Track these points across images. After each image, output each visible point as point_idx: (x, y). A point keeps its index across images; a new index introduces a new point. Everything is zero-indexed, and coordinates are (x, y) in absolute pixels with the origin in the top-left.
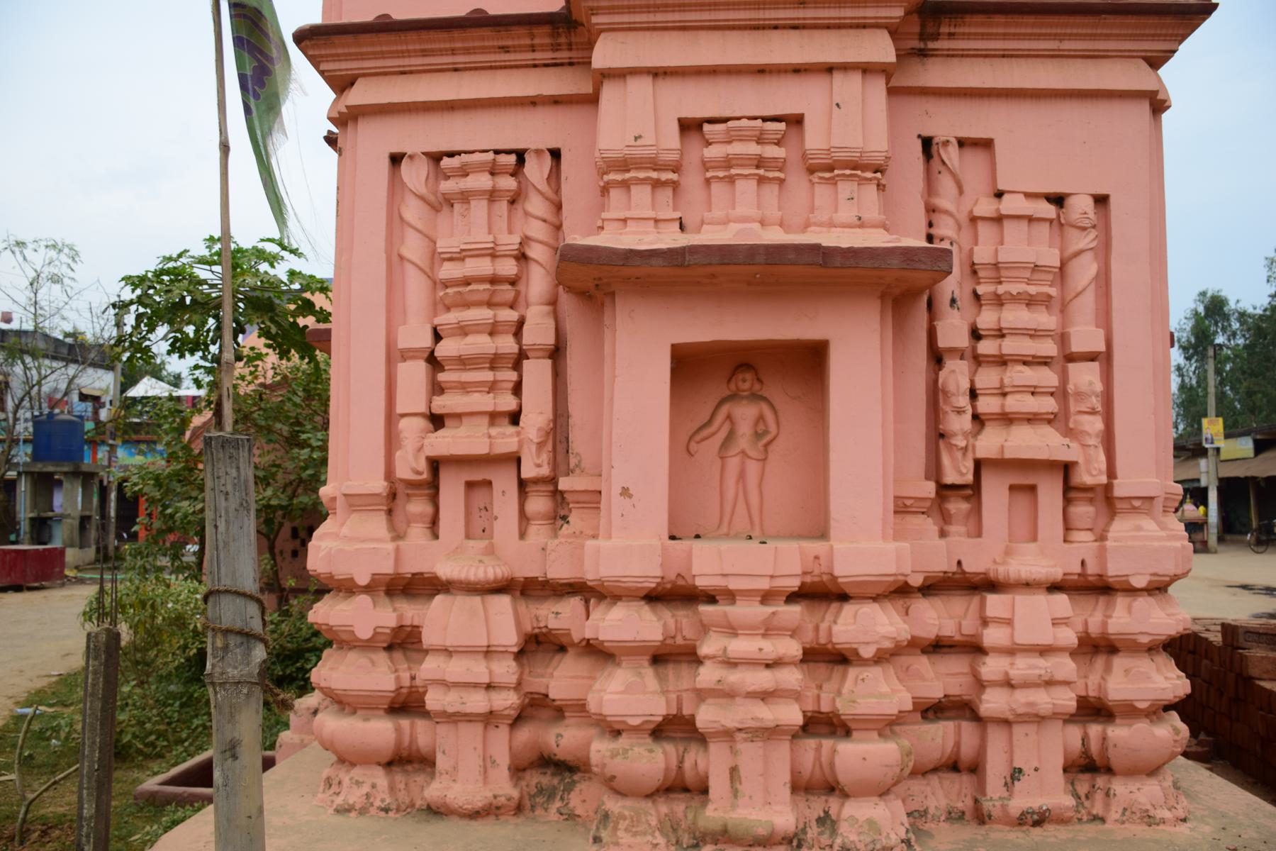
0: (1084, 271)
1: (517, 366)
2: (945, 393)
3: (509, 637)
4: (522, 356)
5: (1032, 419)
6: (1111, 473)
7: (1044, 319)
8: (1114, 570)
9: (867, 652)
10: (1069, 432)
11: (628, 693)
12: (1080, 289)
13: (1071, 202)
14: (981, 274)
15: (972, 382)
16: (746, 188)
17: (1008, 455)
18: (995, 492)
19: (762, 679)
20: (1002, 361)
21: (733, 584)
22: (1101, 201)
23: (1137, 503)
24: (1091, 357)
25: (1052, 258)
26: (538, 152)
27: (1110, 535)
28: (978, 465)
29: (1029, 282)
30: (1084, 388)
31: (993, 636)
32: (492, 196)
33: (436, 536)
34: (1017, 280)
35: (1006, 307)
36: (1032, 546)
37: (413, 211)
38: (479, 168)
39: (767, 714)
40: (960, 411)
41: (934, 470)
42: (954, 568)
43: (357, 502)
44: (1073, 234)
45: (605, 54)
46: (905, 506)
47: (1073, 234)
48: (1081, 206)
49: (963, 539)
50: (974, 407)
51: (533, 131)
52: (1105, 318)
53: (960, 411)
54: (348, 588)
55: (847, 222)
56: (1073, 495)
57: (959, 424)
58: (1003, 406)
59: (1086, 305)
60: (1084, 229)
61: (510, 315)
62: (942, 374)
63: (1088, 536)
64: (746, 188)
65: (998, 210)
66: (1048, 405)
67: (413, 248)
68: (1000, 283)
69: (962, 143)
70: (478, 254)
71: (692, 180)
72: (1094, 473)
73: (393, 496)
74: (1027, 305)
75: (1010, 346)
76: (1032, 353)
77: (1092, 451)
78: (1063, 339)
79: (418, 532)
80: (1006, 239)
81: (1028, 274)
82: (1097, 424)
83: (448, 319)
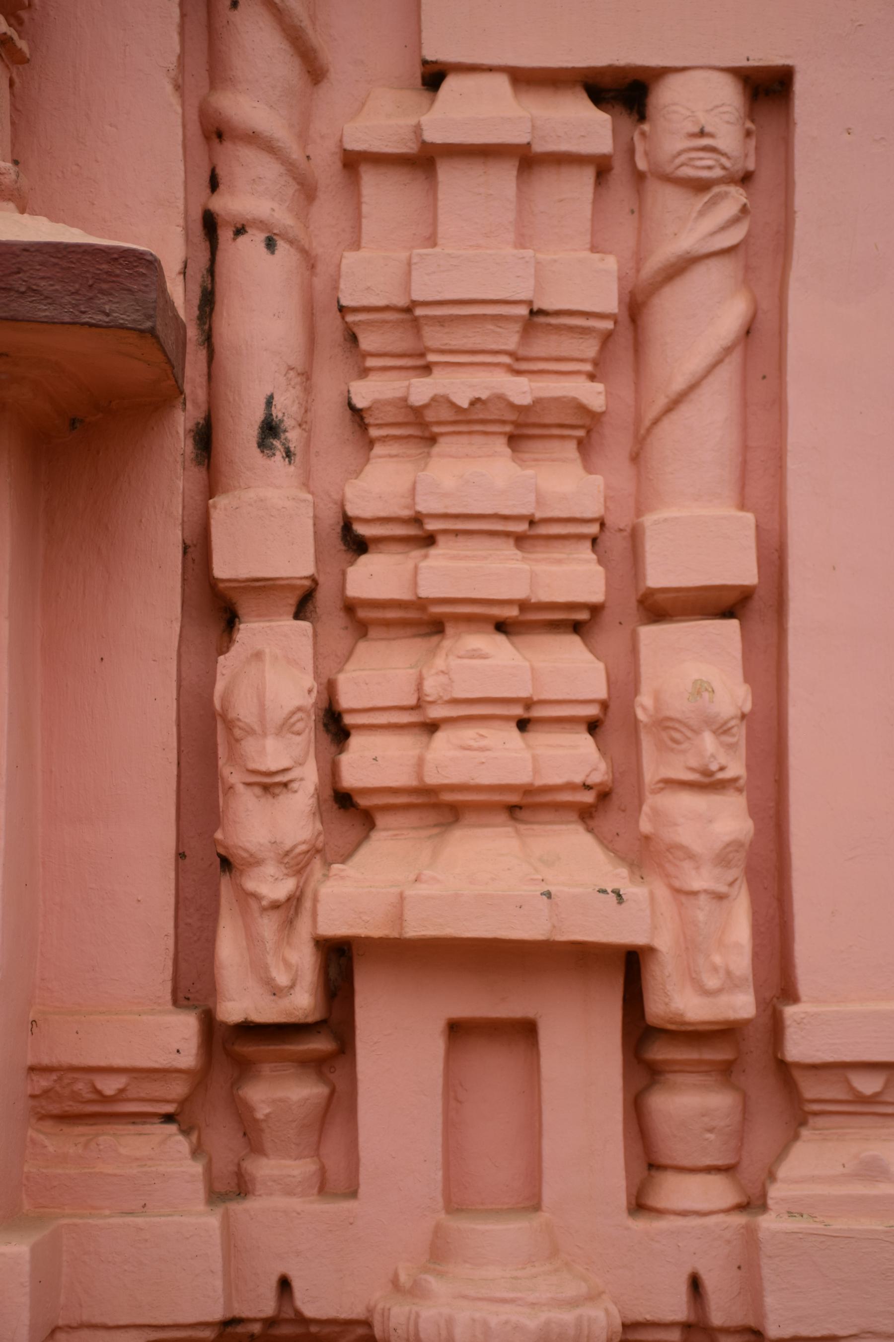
0: (701, 322)
2: (230, 725)
5: (521, 805)
6: (779, 982)
7: (565, 484)
10: (645, 855)
12: (679, 384)
13: (668, 97)
14: (367, 342)
15: (330, 689)
17: (414, 930)
18: (399, 1045)
20: (429, 621)
22: (767, 90)
23: (868, 1084)
24: (729, 604)
25: (590, 284)
27: (775, 1192)
28: (339, 958)
29: (518, 363)
30: (679, 706)
34: (474, 358)
35: (444, 446)
36: (512, 1231)
40: (271, 785)
41: (193, 984)
42: (265, 1304)
44: (668, 201)
46: (105, 1099)
47: (668, 201)
48: (699, 109)
49: (295, 1203)
50: (332, 771)
52: (761, 475)
53: (271, 785)
56: (660, 1053)
57: (272, 826)
58: (420, 763)
59: (701, 437)
60: (700, 186)
62: (227, 663)
63: (715, 1192)
65: (418, 129)
66: (572, 759)
68: (427, 369)
72: (712, 982)
74: (513, 440)
76: (519, 592)
77: (702, 911)
78: (613, 539)
80: (447, 225)
81: (510, 339)
82: (728, 820)
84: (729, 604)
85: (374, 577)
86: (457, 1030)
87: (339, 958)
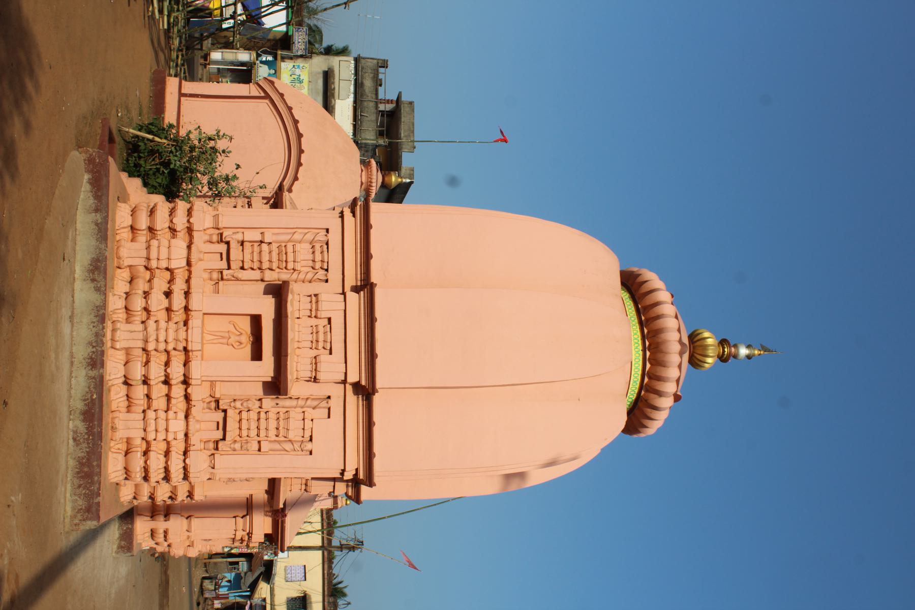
0: (288, 446)
1: (260, 269)
3: (173, 266)
7: (272, 433)
8: (191, 454)
16: (310, 337)
19: (162, 339)
21: (189, 331)
24: (259, 450)
25: (291, 435)
26: (326, 275)
31: (171, 413)
32: (314, 261)
37: (309, 237)
38: (323, 257)
39: (152, 338)
43: (216, 217)
45: (352, 297)
48: (309, 446)
51: (335, 275)
54: (190, 212)
57: (238, 404)
61: (274, 266)
64: (310, 337)
67: (297, 237)
69: (329, 409)
70: (295, 257)
71: (314, 321)
73: (218, 229)
75: (263, 421)
83: (274, 246)
84: (259, 450)
85: (263, 415)
86: (218, 423)
87: (225, 411)
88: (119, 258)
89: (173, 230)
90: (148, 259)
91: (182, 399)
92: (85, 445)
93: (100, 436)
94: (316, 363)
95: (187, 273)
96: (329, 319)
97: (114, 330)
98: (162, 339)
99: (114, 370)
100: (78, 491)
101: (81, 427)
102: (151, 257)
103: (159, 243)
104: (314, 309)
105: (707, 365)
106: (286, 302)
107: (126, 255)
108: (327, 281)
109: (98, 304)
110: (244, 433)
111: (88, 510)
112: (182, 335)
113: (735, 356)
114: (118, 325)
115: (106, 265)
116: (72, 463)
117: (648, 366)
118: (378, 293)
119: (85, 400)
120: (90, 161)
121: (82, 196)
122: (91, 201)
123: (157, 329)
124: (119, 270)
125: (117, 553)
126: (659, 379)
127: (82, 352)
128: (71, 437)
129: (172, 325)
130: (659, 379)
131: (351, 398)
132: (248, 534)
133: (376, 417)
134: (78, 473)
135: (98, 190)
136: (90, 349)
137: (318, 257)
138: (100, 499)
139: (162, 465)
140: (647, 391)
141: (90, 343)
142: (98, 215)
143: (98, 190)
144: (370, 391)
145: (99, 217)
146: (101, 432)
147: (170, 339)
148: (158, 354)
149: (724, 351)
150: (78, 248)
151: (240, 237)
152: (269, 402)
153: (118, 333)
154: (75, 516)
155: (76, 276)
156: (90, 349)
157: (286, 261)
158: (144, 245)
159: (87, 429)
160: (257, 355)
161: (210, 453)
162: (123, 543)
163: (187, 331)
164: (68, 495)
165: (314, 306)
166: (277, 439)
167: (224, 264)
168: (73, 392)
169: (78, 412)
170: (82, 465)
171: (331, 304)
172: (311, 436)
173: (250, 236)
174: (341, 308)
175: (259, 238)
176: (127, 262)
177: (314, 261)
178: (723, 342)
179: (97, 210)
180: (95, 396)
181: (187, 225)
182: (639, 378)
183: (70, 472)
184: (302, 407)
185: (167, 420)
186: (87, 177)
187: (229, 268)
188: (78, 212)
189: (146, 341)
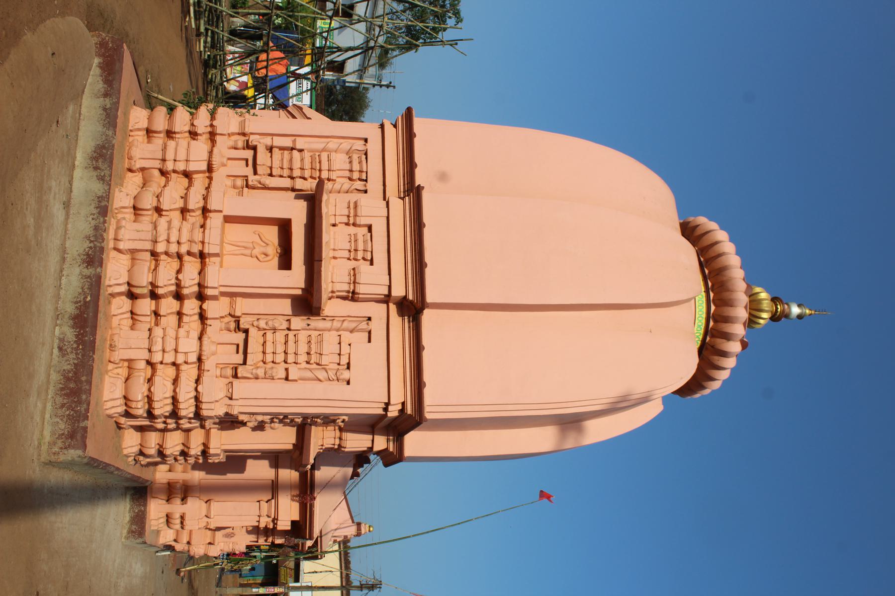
0: (321, 375)
4: (292, 178)
7: (302, 358)
9: (180, 276)
11: (172, 198)
19: (173, 239)
25: (325, 360)
26: (365, 186)
32: (351, 171)
33: (230, 148)
38: (361, 167)
43: (243, 124)
48: (346, 375)
51: (375, 184)
55: (334, 275)
69: (370, 332)
71: (352, 230)
73: (244, 134)
79: (230, 142)
86: (238, 345)
87: (246, 331)
88: (130, 158)
89: (193, 135)
90: (164, 160)
91: (197, 317)
92: (73, 356)
93: (93, 348)
94: (355, 275)
95: (207, 181)
96: (370, 228)
97: (118, 228)
98: (173, 239)
99: (116, 272)
100: (60, 412)
101: (70, 334)
102: (167, 158)
103: (177, 145)
104: (352, 215)
105: (761, 321)
106: (321, 202)
107: (138, 156)
108: (366, 192)
109: (100, 194)
110: (269, 358)
111: (72, 435)
112: (198, 236)
113: (786, 315)
114: (123, 223)
115: (112, 154)
116: (55, 377)
117: (713, 308)
118: (426, 196)
119: (76, 303)
120: (102, 44)
121: (89, 80)
122: (100, 86)
123: (169, 228)
124: (130, 174)
125: (127, 538)
126: (727, 320)
127: (77, 247)
128: (56, 346)
129: (186, 226)
130: (727, 320)
131: (396, 321)
132: (273, 521)
133: (425, 341)
134: (62, 389)
135: (109, 74)
136: (87, 244)
137: (356, 167)
138: (88, 423)
139: (169, 394)
140: (713, 336)
141: (88, 238)
142: (107, 100)
143: (109, 74)
144: (420, 305)
145: (108, 102)
146: (94, 342)
147: (184, 240)
148: (169, 260)
149: (777, 308)
150: (80, 134)
151: (268, 141)
152: (298, 322)
153: (122, 231)
154: (55, 443)
155: (77, 163)
156: (87, 244)
157: (320, 170)
158: (160, 148)
159: (77, 336)
160: (285, 263)
161: (227, 381)
162: (134, 527)
163: (204, 232)
164: (47, 416)
165: (352, 211)
166: (308, 366)
167: (249, 171)
168: (62, 292)
169: (67, 316)
170: (68, 379)
171: (371, 208)
172: (349, 364)
173: (279, 142)
174: (382, 210)
175: (290, 145)
176: (139, 164)
177: (351, 171)
178: (775, 300)
179: (106, 95)
180: (89, 298)
181: (209, 129)
182: (704, 321)
183: (51, 388)
184: (338, 330)
185: (177, 338)
186: (96, 61)
187: (255, 173)
188: (84, 97)
189: (155, 242)
